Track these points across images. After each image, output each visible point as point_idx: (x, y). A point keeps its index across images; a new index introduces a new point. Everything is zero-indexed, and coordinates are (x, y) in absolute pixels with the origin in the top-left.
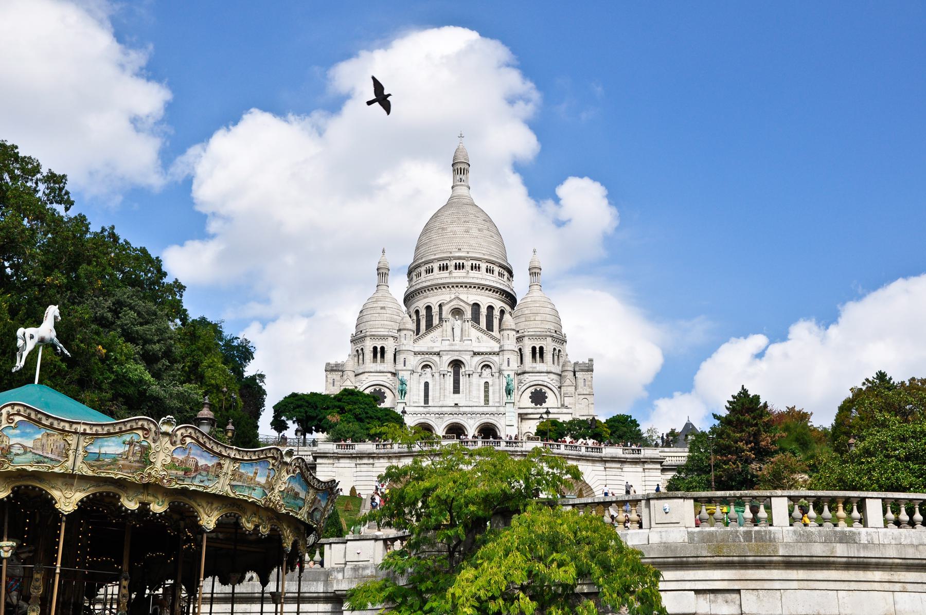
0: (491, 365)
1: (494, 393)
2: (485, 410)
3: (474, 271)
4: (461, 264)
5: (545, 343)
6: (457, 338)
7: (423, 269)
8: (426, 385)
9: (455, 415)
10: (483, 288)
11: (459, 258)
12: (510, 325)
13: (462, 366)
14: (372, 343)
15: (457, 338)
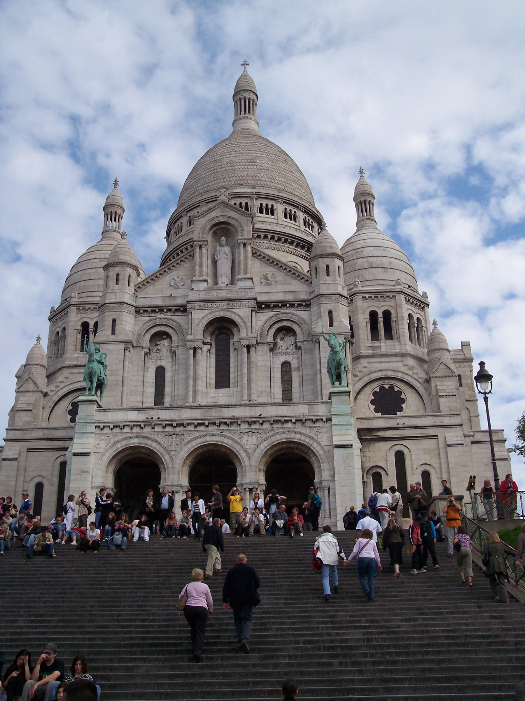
0: (295, 327)
1: (302, 384)
2: (280, 413)
3: (264, 215)
4: (244, 205)
5: (392, 303)
6: (224, 280)
7: (184, 220)
8: (160, 372)
9: (211, 428)
10: (279, 239)
11: (240, 195)
12: (331, 247)
13: (235, 330)
14: (79, 316)
15: (224, 280)
